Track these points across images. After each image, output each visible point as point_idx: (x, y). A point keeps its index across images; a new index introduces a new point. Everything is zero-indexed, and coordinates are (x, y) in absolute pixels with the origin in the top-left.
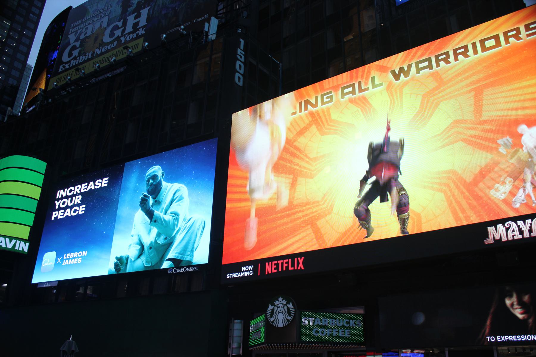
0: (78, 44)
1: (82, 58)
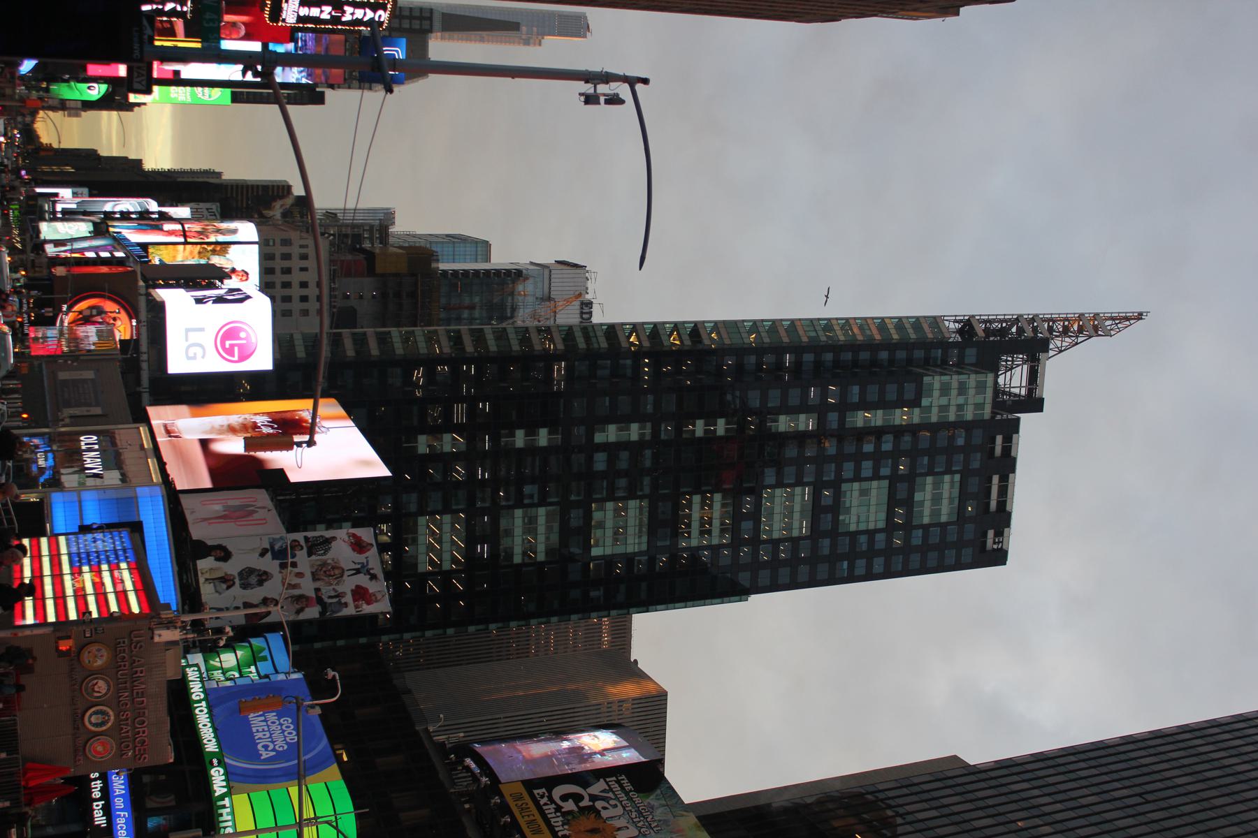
0: (586, 803)
1: (557, 821)
